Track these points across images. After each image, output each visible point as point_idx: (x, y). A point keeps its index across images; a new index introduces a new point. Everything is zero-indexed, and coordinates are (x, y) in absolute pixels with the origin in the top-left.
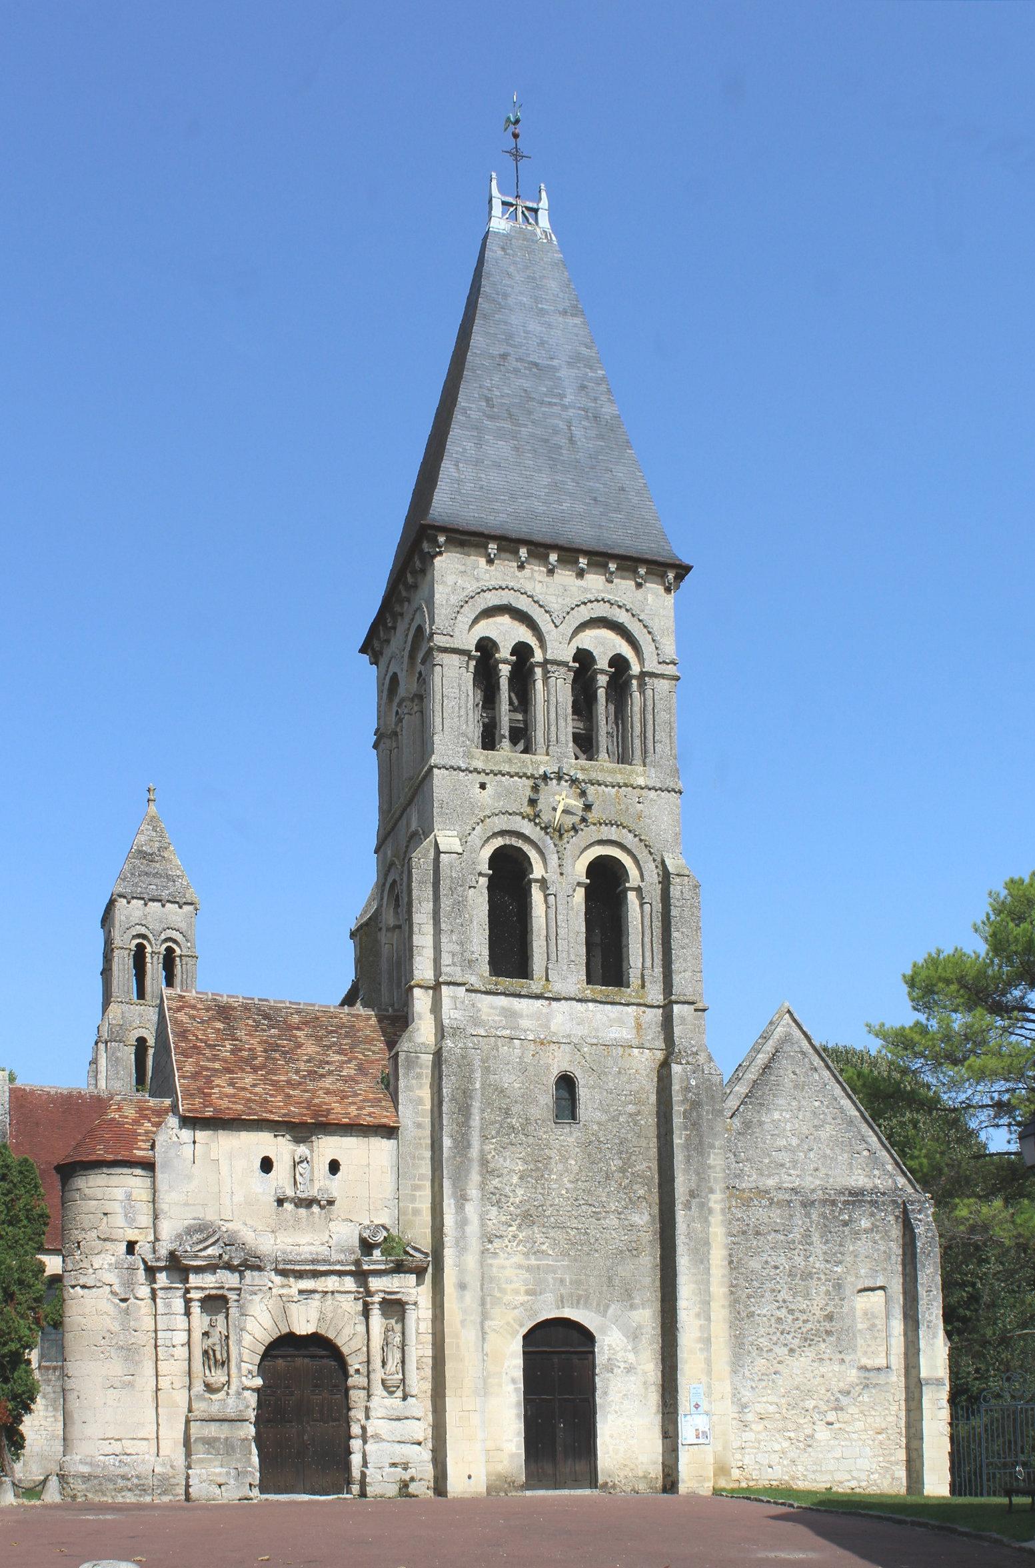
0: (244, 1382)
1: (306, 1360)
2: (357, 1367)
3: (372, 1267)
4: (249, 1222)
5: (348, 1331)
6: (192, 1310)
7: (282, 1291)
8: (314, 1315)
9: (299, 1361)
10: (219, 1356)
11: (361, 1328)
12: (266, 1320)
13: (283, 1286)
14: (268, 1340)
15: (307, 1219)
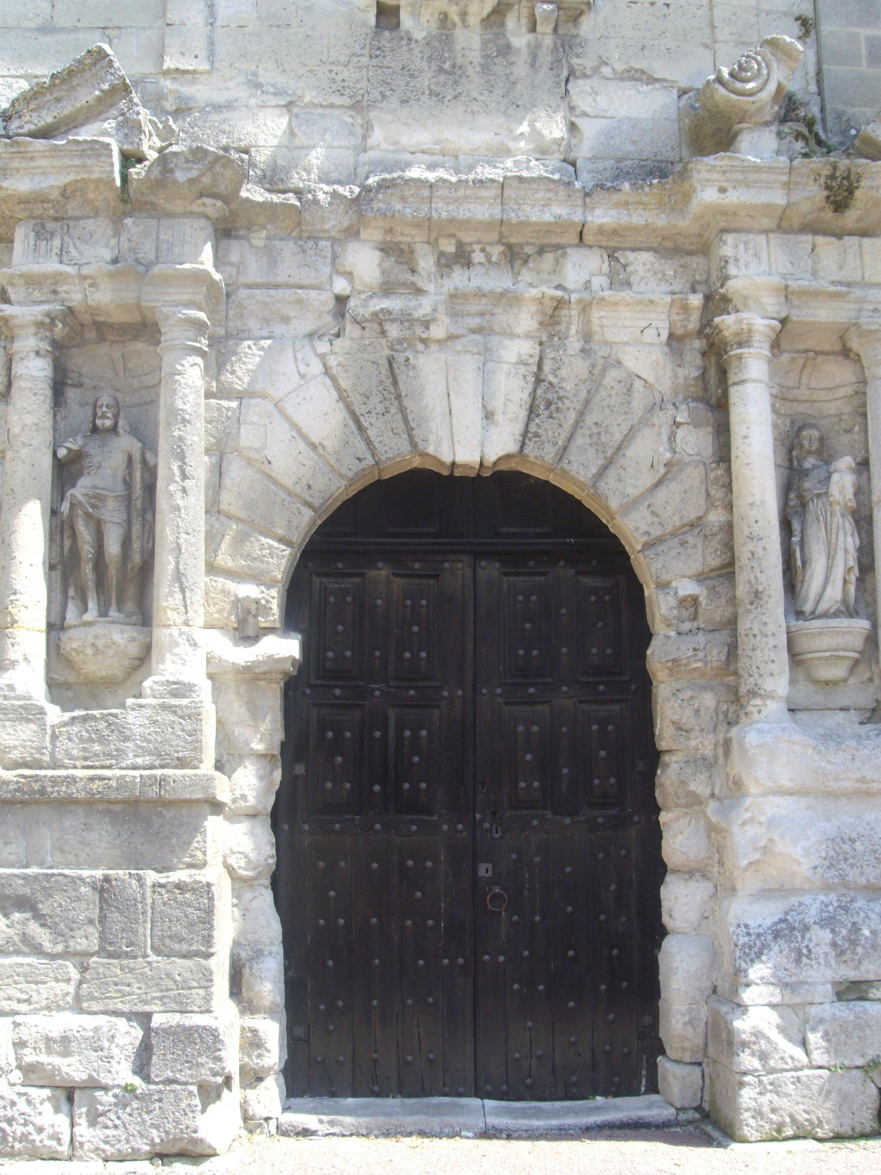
0: (218, 645)
1: (490, 570)
2: (687, 588)
3: (734, 197)
4: (269, 75)
5: (648, 448)
6: (19, 369)
7: (394, 304)
8: (512, 391)
9: (458, 571)
10: (113, 548)
11: (695, 441)
12: (320, 413)
13: (387, 289)
14: (333, 488)
15: (485, 68)
